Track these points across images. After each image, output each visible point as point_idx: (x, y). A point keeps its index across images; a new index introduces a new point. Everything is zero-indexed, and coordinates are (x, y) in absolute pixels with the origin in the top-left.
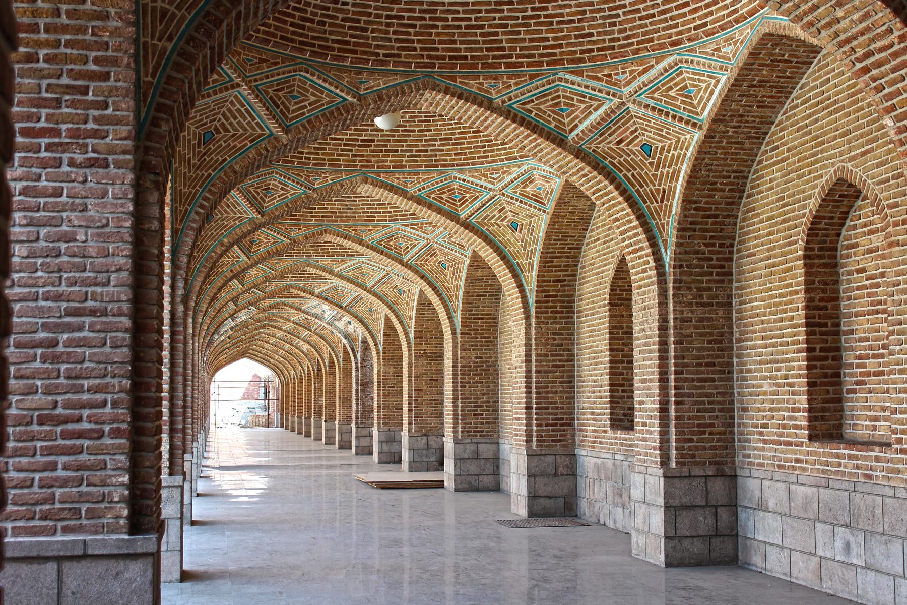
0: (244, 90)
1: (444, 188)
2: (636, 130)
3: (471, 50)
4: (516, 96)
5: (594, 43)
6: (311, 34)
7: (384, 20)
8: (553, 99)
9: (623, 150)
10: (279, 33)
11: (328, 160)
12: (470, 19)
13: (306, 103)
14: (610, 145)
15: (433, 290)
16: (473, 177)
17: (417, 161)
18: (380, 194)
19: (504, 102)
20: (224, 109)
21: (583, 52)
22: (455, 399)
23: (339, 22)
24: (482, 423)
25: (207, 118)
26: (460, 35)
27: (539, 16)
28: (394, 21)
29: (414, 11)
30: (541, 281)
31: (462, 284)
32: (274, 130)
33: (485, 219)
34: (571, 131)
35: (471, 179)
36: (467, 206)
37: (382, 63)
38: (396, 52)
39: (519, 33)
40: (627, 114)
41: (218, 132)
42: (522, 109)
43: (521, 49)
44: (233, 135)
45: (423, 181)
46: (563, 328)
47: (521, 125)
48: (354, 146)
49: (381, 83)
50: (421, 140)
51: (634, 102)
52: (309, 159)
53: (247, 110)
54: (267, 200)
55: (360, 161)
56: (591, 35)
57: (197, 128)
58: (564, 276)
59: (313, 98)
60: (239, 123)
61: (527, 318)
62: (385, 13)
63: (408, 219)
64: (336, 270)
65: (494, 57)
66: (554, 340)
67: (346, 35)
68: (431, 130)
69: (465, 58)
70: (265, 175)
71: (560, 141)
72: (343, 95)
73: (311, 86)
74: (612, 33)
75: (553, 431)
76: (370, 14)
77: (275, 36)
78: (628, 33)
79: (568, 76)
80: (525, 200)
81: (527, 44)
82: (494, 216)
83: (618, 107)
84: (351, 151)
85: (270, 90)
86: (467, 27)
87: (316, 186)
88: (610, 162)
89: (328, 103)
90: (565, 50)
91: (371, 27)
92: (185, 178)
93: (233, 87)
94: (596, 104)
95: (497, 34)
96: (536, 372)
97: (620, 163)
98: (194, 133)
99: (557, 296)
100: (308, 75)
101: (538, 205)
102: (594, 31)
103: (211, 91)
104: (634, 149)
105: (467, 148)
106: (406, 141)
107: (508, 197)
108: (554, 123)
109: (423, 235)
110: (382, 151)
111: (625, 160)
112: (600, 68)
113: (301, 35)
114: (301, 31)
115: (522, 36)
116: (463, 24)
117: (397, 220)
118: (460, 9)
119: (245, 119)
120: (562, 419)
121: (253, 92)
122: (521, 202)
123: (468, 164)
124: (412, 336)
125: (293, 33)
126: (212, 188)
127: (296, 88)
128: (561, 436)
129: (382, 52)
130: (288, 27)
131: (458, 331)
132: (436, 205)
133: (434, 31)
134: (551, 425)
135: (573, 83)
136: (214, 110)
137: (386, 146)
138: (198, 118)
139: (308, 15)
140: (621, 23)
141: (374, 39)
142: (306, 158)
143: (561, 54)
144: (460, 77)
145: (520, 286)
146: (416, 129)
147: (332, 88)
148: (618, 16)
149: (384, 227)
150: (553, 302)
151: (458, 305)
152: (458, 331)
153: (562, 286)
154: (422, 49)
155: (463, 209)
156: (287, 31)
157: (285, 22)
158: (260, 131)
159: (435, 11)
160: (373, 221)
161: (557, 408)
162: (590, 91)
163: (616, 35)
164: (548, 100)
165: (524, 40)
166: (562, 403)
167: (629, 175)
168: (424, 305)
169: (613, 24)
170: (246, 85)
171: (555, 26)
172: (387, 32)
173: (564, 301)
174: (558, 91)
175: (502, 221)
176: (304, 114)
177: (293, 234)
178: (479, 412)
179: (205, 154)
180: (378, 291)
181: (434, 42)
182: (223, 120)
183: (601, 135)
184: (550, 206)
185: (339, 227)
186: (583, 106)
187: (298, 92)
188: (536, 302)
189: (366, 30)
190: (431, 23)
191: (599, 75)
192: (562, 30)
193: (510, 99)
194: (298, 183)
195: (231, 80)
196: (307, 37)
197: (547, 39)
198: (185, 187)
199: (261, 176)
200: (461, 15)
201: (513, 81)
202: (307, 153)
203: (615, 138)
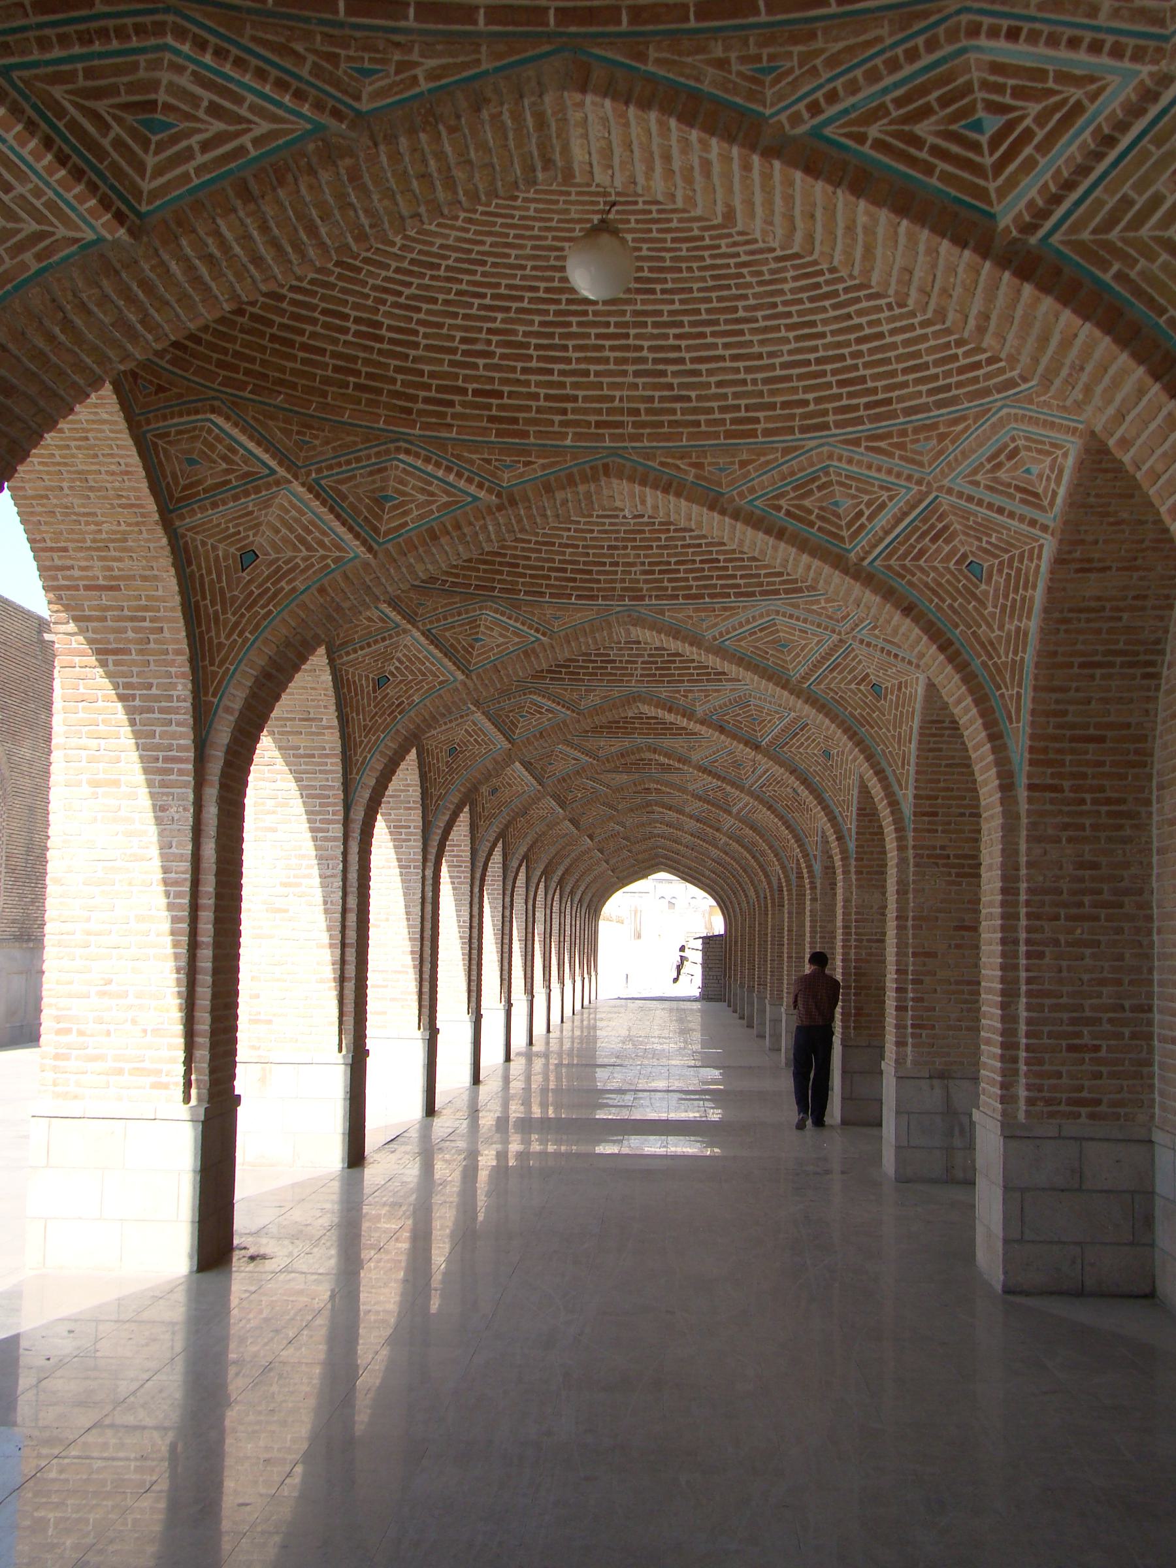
1: (923, 90)
15: (942, 649)
22: (1009, 994)
24: (1098, 1076)
31: (1033, 625)
33: (1111, 222)
45: (832, 62)
54: (151, 161)
63: (859, 421)
64: (708, 635)
87: (365, 106)
117: (825, 426)
124: (907, 808)
131: (1022, 781)
149: (786, 451)
151: (1020, 698)
152: (1022, 781)
155: (1012, 183)
160: (753, 434)
168: (940, 727)
177: (506, 478)
178: (1087, 1040)
194: (281, 85)
199: (104, 34)
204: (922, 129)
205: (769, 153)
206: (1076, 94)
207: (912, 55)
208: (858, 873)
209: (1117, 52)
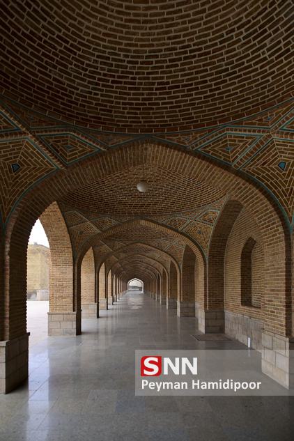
4: (200, 143)
5: (250, 103)
8: (222, 143)
12: (172, 103)
19: (193, 148)
26: (166, 112)
29: (138, 99)
30: (210, 251)
34: (233, 161)
37: (121, 130)
39: (202, 107)
40: (271, 144)
42: (204, 151)
47: (203, 160)
59: (81, 149)
60: (35, 161)
61: (205, 265)
71: (226, 167)
72: (98, 147)
73: (78, 141)
83: (266, 139)
85: (50, 140)
86: (171, 108)
93: (21, 133)
95: (189, 110)
100: (75, 135)
108: (223, 157)
113: (68, 111)
118: (166, 96)
121: (37, 139)
125: (63, 108)
129: (121, 124)
135: (236, 130)
139: (73, 100)
141: (116, 117)
145: (202, 254)
147: (92, 143)
154: (145, 122)
159: (151, 99)
162: (247, 133)
165: (205, 111)
172: (124, 113)
176: (76, 157)
183: (252, 161)
186: (241, 144)
191: (254, 121)
193: (197, 145)
195: (19, 129)
200: (167, 101)
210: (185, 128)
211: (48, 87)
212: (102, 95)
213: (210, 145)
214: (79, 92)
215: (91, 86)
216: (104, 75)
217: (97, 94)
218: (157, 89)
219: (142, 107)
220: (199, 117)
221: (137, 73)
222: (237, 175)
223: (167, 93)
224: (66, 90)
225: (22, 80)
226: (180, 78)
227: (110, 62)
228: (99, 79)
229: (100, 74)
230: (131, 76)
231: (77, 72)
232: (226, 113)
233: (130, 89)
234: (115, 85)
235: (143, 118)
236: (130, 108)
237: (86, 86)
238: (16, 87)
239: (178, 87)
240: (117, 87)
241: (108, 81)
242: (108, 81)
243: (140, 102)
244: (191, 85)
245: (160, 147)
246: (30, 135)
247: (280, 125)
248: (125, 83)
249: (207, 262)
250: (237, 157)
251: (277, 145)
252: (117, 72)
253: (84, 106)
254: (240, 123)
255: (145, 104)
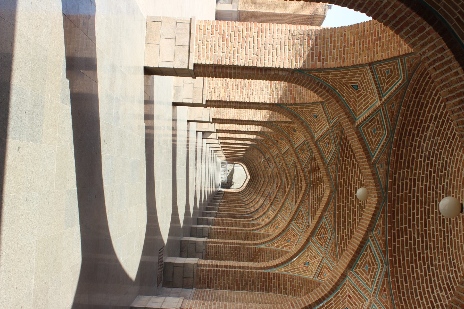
0: (378, 103)
2: (356, 305)
3: (398, 221)
5: (402, 284)
6: (406, 139)
7: (413, 177)
8: (372, 262)
9: (345, 298)
10: (406, 122)
11: (342, 174)
12: (414, 221)
13: (371, 137)
14: (348, 292)
16: (332, 244)
17: (340, 217)
18: (325, 200)
20: (369, 95)
21: (397, 278)
22: (225, 243)
23: (412, 154)
25: (365, 85)
26: (406, 216)
27: (416, 256)
28: (413, 183)
29: (418, 192)
32: (358, 121)
35: (331, 243)
36: (318, 241)
38: (397, 183)
39: (407, 246)
40: (364, 300)
41: (358, 92)
42: (368, 247)
43: (398, 247)
44: (356, 101)
45: (331, 220)
46: (255, 286)
48: (348, 187)
49: (381, 174)
50: (350, 219)
51: (371, 303)
52: (342, 165)
53: (368, 106)
54: (323, 144)
55: (341, 190)
56: (406, 283)
57: (360, 81)
58: (281, 288)
59: (374, 140)
62: (417, 178)
65: (394, 233)
66: (250, 281)
67: (406, 157)
68: (355, 224)
69: (394, 219)
70: (335, 143)
72: (375, 155)
74: (408, 293)
75: (205, 278)
76: (416, 170)
77: (405, 120)
78: (407, 301)
79: (384, 271)
80: (320, 268)
81: (401, 250)
82: (312, 254)
84: (346, 186)
85: (378, 117)
87: (329, 168)
88: (339, 292)
89: (371, 148)
90: (398, 269)
91: (409, 170)
92: (336, 76)
93: (380, 97)
94: (370, 284)
95: (406, 235)
96: (235, 271)
97: (339, 297)
98: (357, 80)
99: (271, 284)
100: (385, 137)
101: (317, 274)
102: (408, 284)
103: (378, 85)
104: (346, 304)
105: (346, 241)
106: (350, 212)
107: (322, 260)
108: (360, 263)
109: (304, 231)
110: (346, 200)
111: (340, 300)
112: (389, 286)
113: (405, 134)
114: (407, 134)
115: (405, 248)
116: (411, 218)
119: (364, 106)
120: (211, 283)
121: (377, 108)
122: (319, 266)
123: (338, 241)
124: (256, 232)
125: (406, 130)
126: (330, 90)
127: (379, 131)
128: (203, 281)
129: (397, 176)
130: (409, 127)
131: (257, 246)
132: (318, 225)
133: (407, 203)
134: (208, 277)
135: (381, 272)
136: (369, 89)
137: (348, 203)
138: (365, 81)
139: (415, 138)
140: (413, 298)
141: (404, 172)
142: (343, 163)
143: (396, 267)
144: (384, 216)
145: (277, 266)
146: (356, 217)
148: (417, 296)
149: (308, 213)
150: (269, 281)
152: (257, 246)
153: (276, 286)
154: (398, 197)
156: (408, 127)
157: (412, 126)
158: (358, 114)
159: (418, 203)
161: (216, 280)
162: (377, 281)
163: (406, 295)
164: (372, 260)
165: (403, 248)
166: (219, 283)
167: (332, 302)
169: (412, 294)
170: (381, 104)
171: (410, 264)
172: (407, 179)
173: (269, 287)
174: (377, 265)
175: (310, 258)
176: (366, 136)
179: (347, 86)
180: (278, 217)
181: (402, 203)
182: (364, 94)
183: (353, 287)
184: (316, 279)
185: (309, 192)
186: (369, 277)
187: (377, 132)
188: (269, 273)
189: (408, 168)
190: (412, 201)
191: (385, 286)
192: (408, 268)
193: (373, 240)
194: (331, 159)
195: (383, 96)
196: (405, 137)
197: (403, 260)
198: (331, 76)
199: (335, 141)
200: (416, 217)
201: (382, 242)
202: (345, 164)
203: (352, 294)
204: (323, 230)
205: (322, 212)
206: (323, 246)
207: (330, 229)
208: (246, 223)
209: (326, 249)
210: (390, 231)
211: (422, 121)
212: (421, 161)
213: (371, 252)
214: (422, 143)
215: (427, 153)
216: (435, 165)
217: (421, 158)
218: (425, 208)
219: (412, 195)
220: (399, 244)
221: (436, 192)
222: (342, 274)
223: (421, 217)
224: (422, 133)
225: (423, 103)
226: (431, 227)
227: (444, 171)
228: (432, 160)
229: (436, 162)
230: (435, 186)
231: (436, 144)
232: (398, 265)
233: (426, 186)
234: (428, 173)
235: (402, 195)
236: (411, 185)
237: (426, 150)
238: (416, 98)
239: (426, 227)
240: (427, 174)
241: (431, 168)
242: (431, 168)
243: (416, 194)
244: (426, 238)
245: (374, 209)
246: (380, 103)
247: (376, 304)
248: (430, 182)
249: (263, 271)
250: (358, 274)
251: (363, 305)
252: (438, 176)
253: (411, 146)
254: (386, 275)
255: (414, 198)
